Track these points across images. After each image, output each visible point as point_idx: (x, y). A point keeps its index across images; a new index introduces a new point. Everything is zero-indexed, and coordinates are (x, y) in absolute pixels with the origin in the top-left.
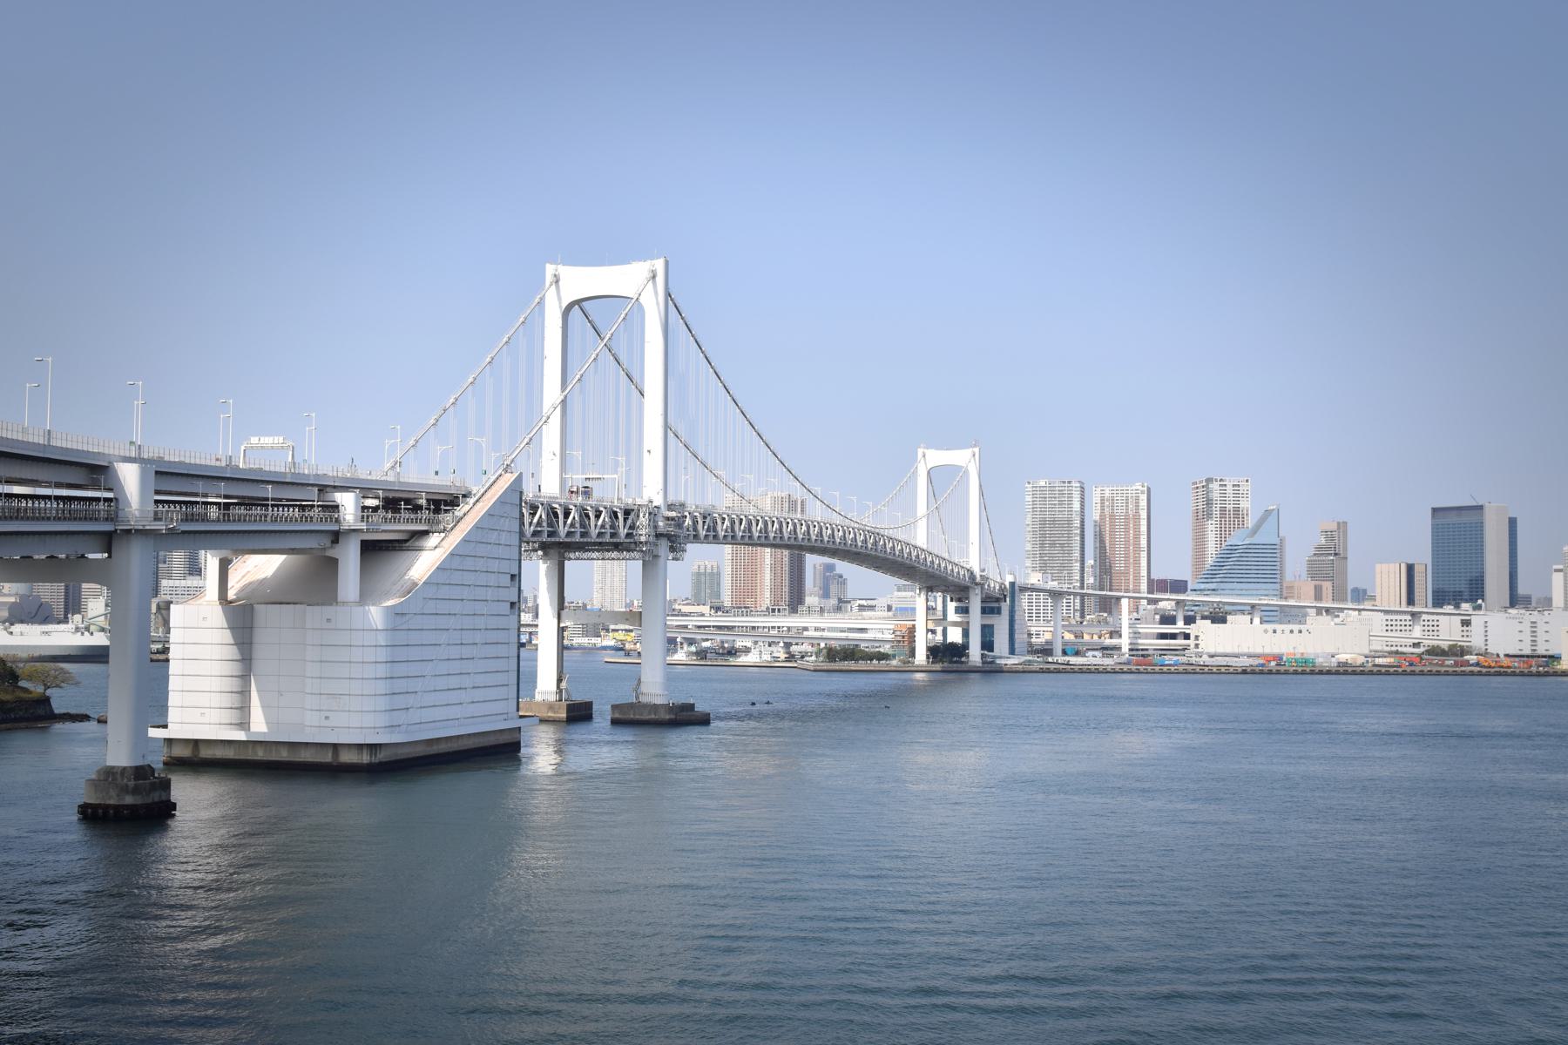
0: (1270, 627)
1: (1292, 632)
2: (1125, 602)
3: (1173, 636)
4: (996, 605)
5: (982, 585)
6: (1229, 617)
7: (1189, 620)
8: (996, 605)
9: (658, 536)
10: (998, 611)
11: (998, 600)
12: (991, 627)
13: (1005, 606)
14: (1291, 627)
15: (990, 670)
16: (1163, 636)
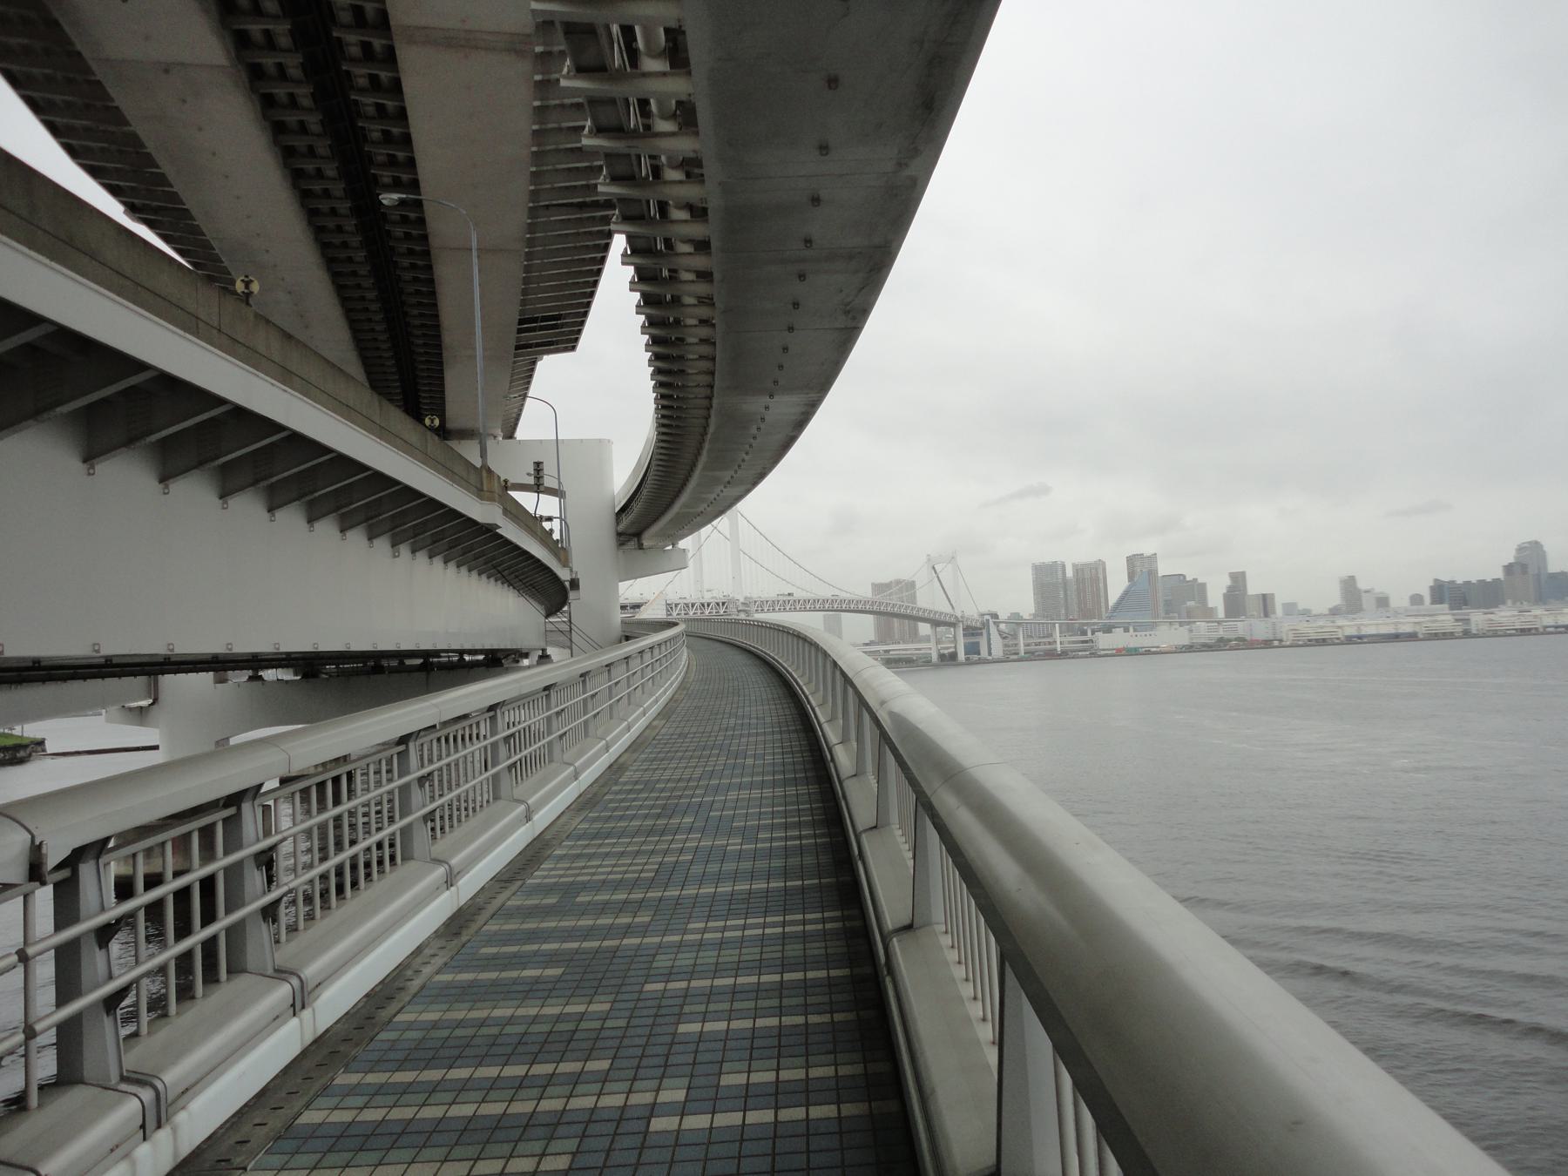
0: (1138, 634)
1: (1146, 635)
2: (1057, 625)
3: (1086, 642)
4: (980, 631)
5: (962, 622)
6: (1113, 630)
7: (1093, 633)
8: (980, 631)
9: (739, 611)
10: (981, 634)
11: (981, 629)
12: (978, 643)
13: (984, 631)
14: (1145, 633)
15: (969, 662)
16: (1083, 642)
